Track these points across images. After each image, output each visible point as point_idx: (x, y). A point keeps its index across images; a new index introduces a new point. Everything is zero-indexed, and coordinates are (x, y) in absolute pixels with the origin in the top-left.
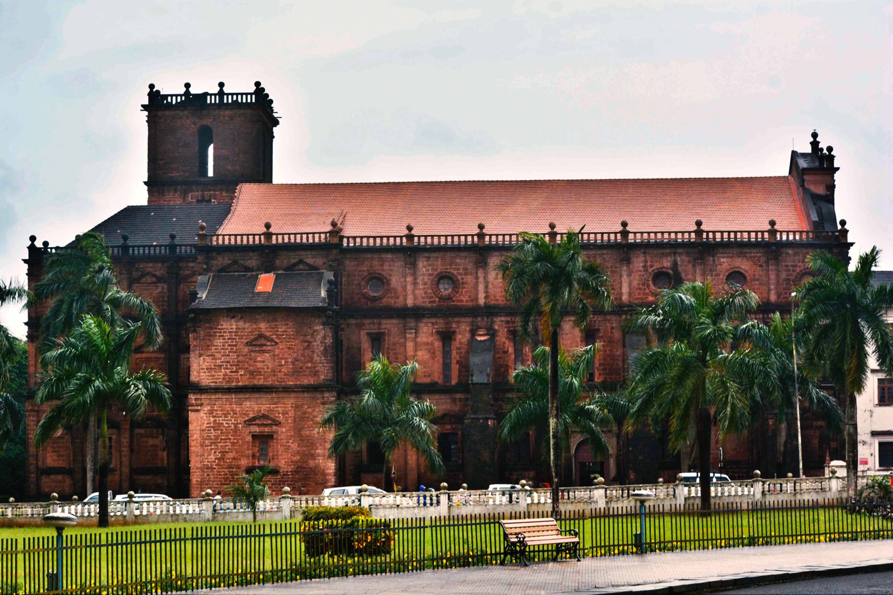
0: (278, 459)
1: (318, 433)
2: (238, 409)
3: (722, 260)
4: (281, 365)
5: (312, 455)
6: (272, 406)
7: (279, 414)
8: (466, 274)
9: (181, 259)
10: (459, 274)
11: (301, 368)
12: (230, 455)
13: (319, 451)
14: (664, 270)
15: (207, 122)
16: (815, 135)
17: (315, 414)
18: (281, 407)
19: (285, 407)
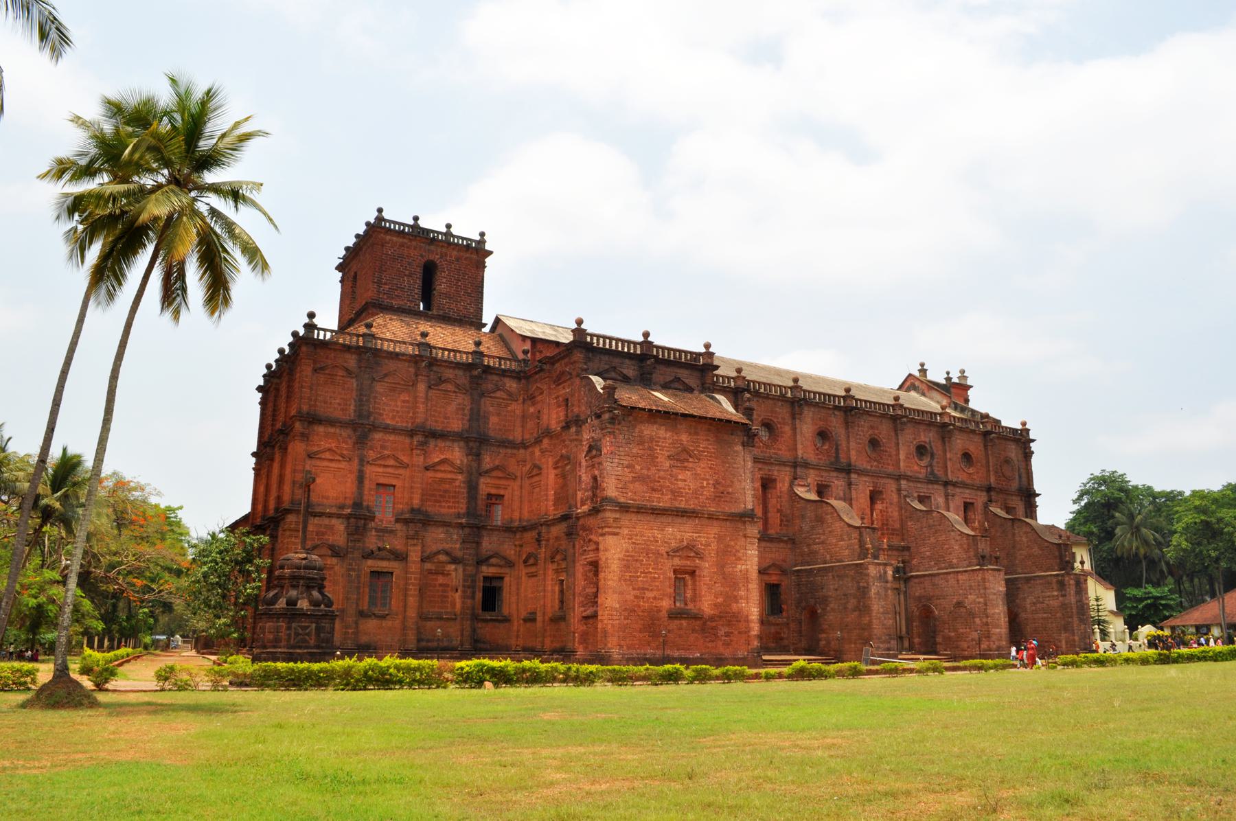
0: (700, 601)
1: (741, 571)
2: (659, 536)
3: (958, 441)
4: (702, 487)
5: (735, 597)
6: (695, 535)
7: (701, 545)
8: (784, 424)
9: (487, 370)
10: (780, 423)
11: (722, 493)
12: (649, 594)
13: (742, 593)
14: (923, 444)
15: (436, 258)
16: (922, 365)
17: (738, 548)
18: (704, 537)
19: (708, 538)
